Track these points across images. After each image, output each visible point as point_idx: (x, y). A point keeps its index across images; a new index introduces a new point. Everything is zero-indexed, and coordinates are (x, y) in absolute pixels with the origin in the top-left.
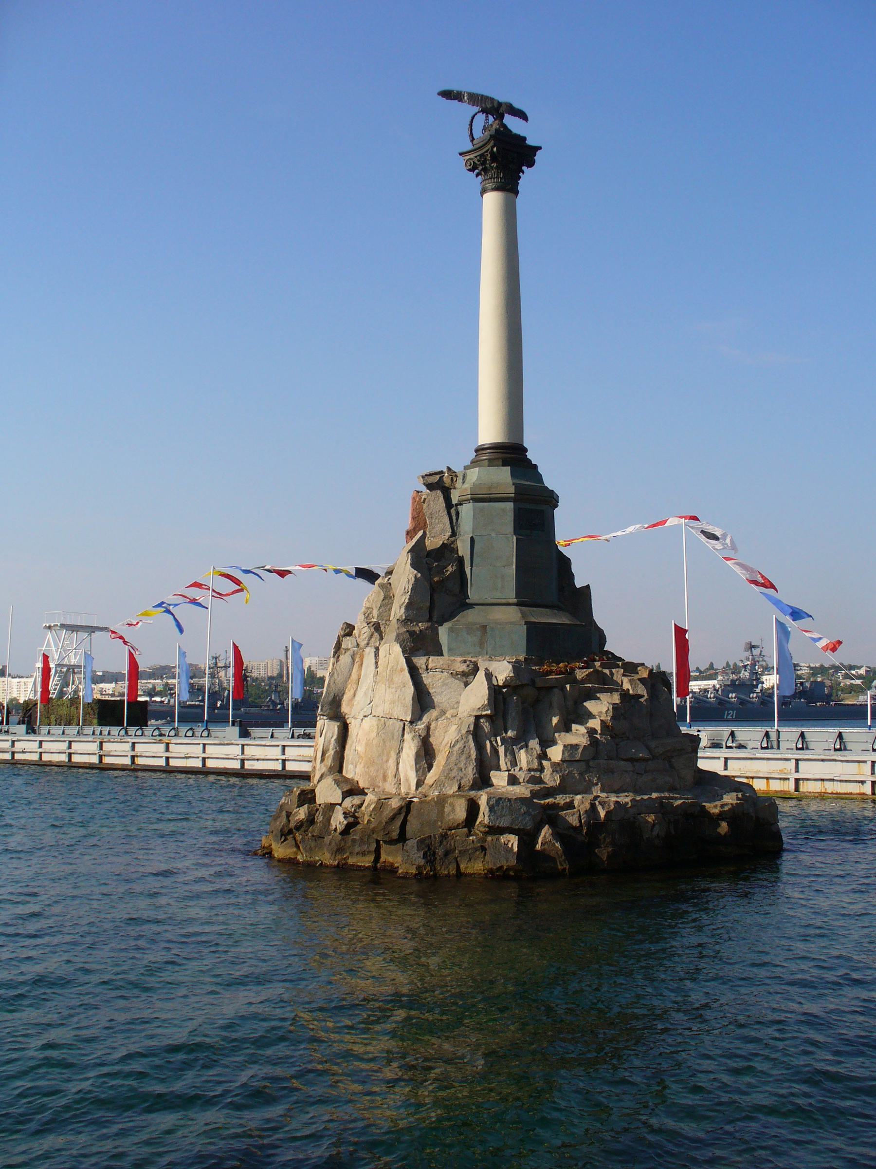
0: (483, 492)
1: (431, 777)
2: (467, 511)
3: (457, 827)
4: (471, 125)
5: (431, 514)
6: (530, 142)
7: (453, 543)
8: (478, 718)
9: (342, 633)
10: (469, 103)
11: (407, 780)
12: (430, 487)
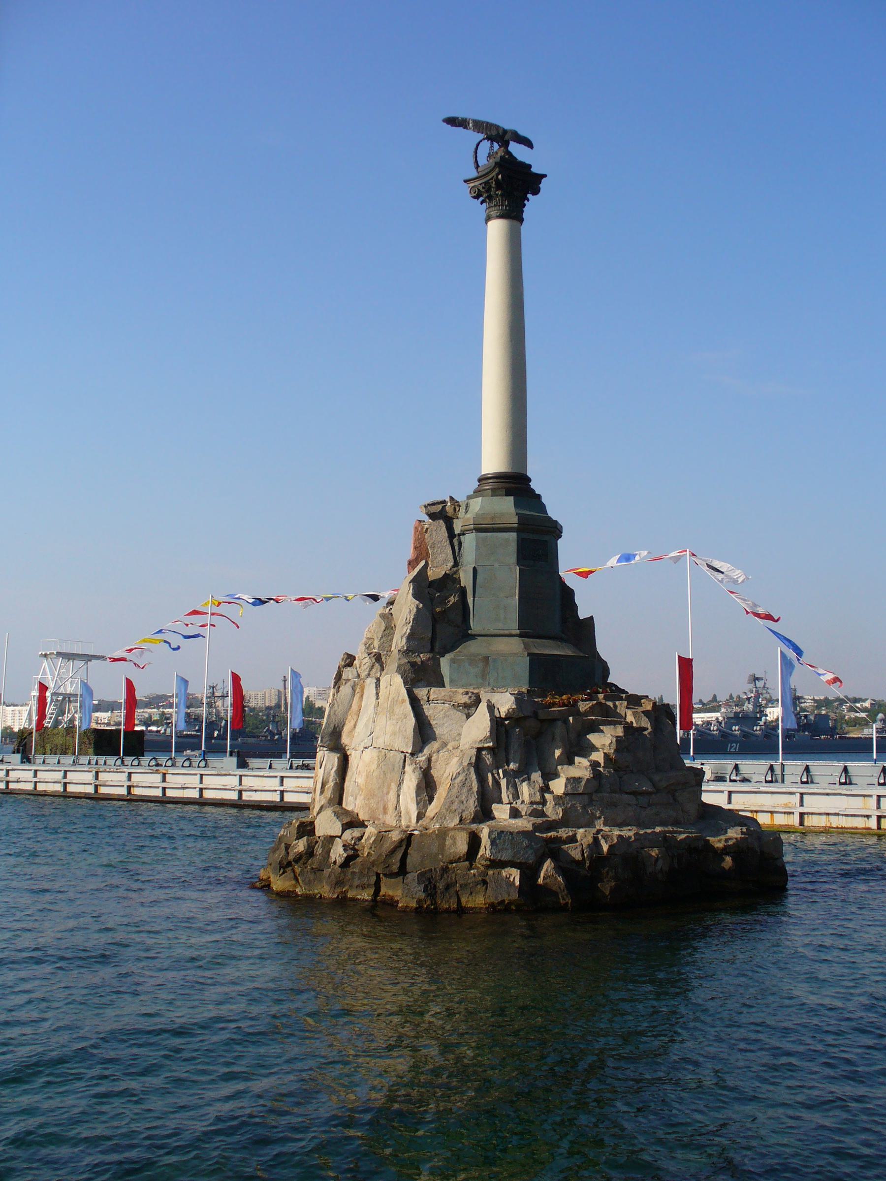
0: (486, 522)
1: (432, 809)
2: (469, 540)
3: (458, 860)
4: (476, 152)
5: (433, 544)
6: (534, 170)
7: (455, 573)
8: (479, 750)
9: (343, 664)
10: (474, 130)
11: (408, 813)
12: (433, 516)
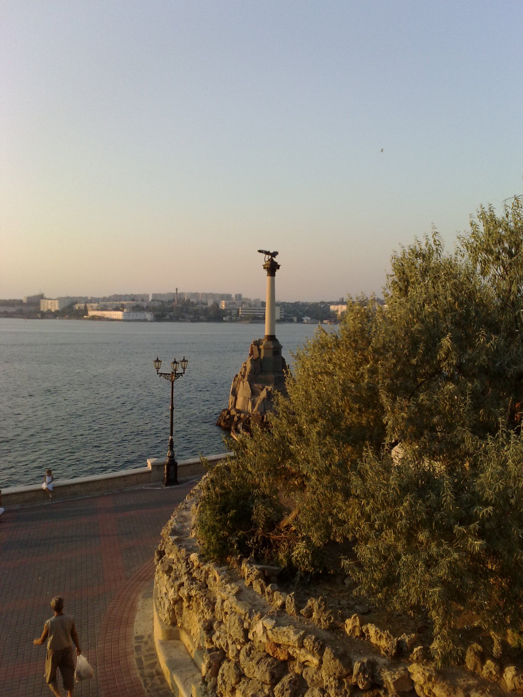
1: (254, 410)
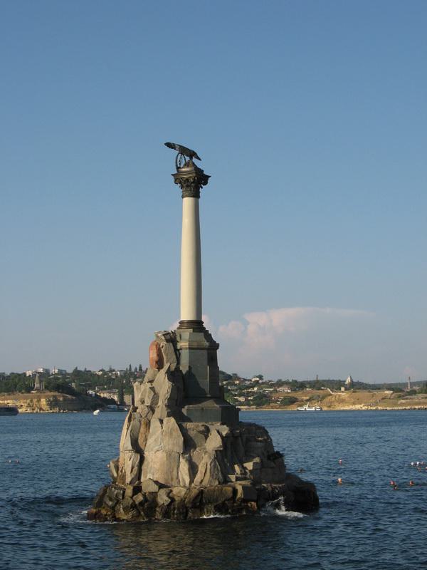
1: (198, 477)
2: (185, 356)
11: (183, 480)
